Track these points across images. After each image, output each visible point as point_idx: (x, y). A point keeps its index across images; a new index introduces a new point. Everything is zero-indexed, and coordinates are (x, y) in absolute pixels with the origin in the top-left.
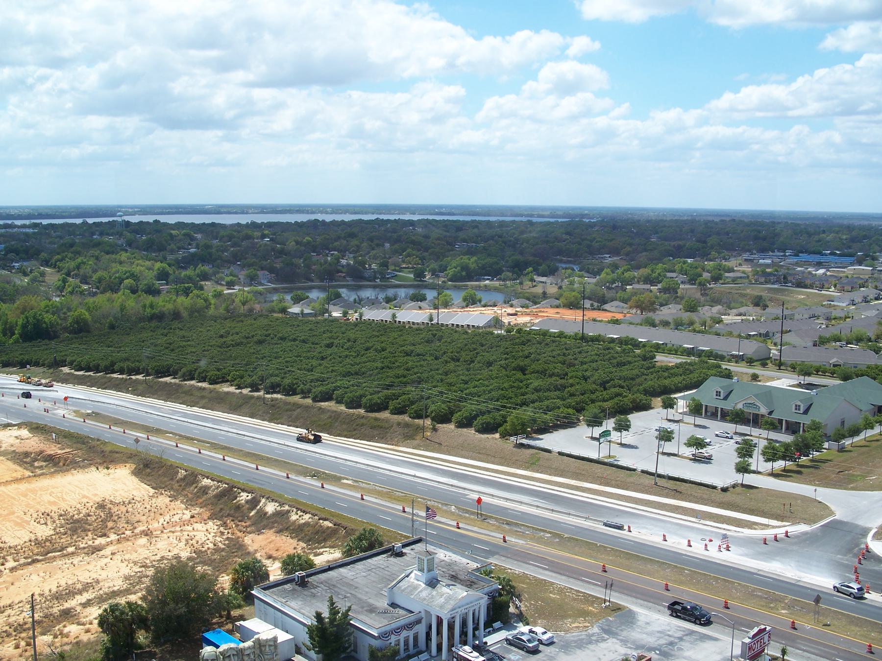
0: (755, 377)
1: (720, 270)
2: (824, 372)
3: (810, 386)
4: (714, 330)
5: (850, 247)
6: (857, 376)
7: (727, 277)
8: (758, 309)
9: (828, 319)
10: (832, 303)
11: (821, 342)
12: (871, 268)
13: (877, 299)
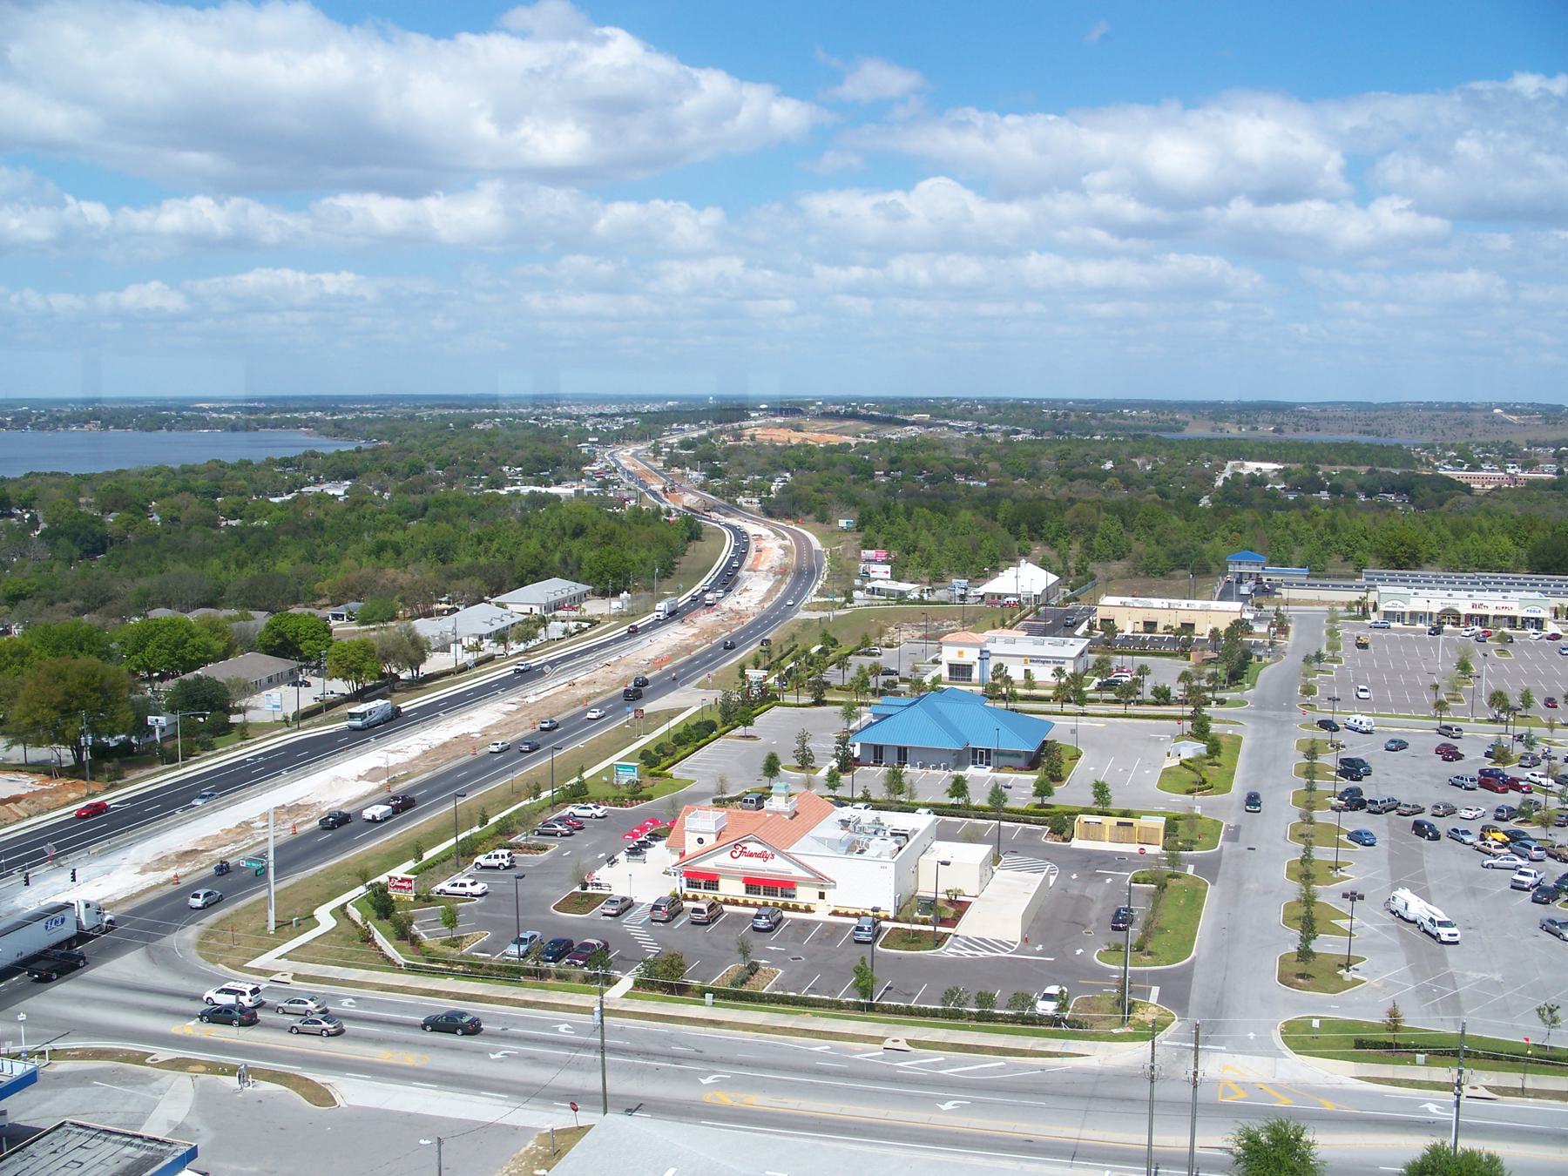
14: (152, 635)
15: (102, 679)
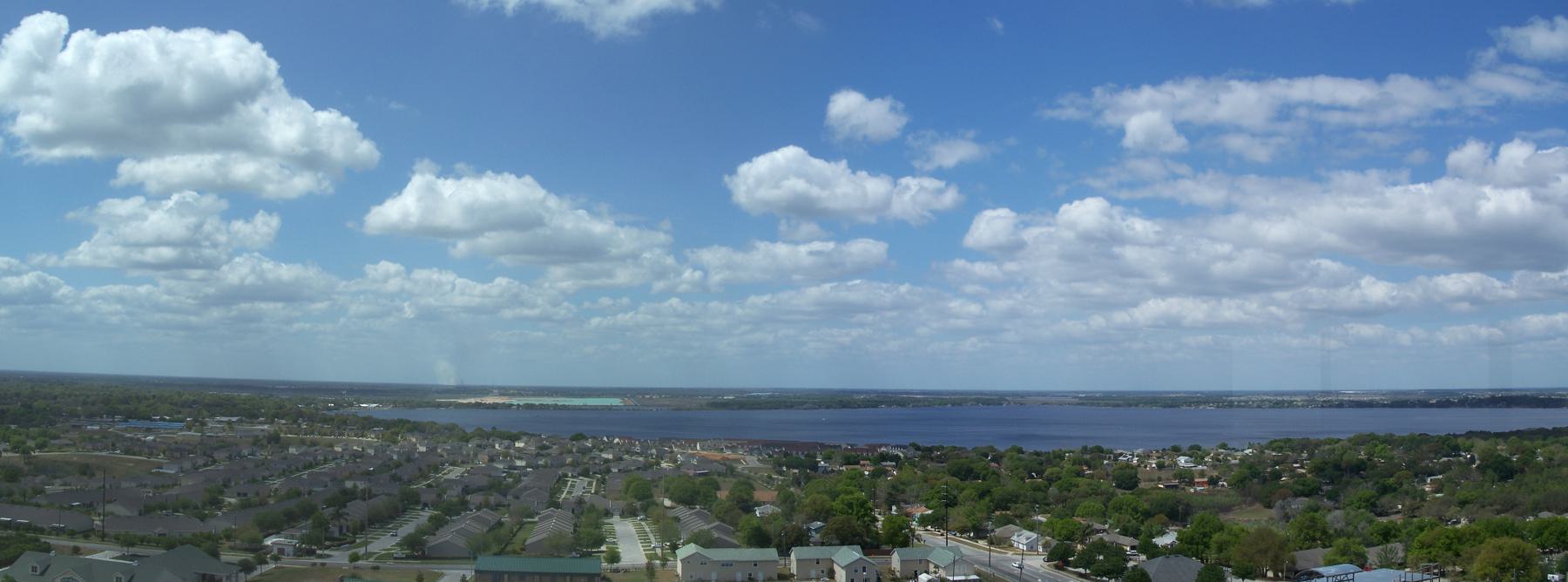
0: (76, 550)
1: (45, 436)
2: (149, 542)
3: (133, 557)
4: (34, 501)
5: (179, 412)
6: (182, 544)
7: (53, 445)
8: (85, 478)
9: (156, 487)
10: (161, 470)
11: (147, 510)
12: (200, 434)
13: (205, 465)
14: (1546, 527)
15: (1523, 551)
